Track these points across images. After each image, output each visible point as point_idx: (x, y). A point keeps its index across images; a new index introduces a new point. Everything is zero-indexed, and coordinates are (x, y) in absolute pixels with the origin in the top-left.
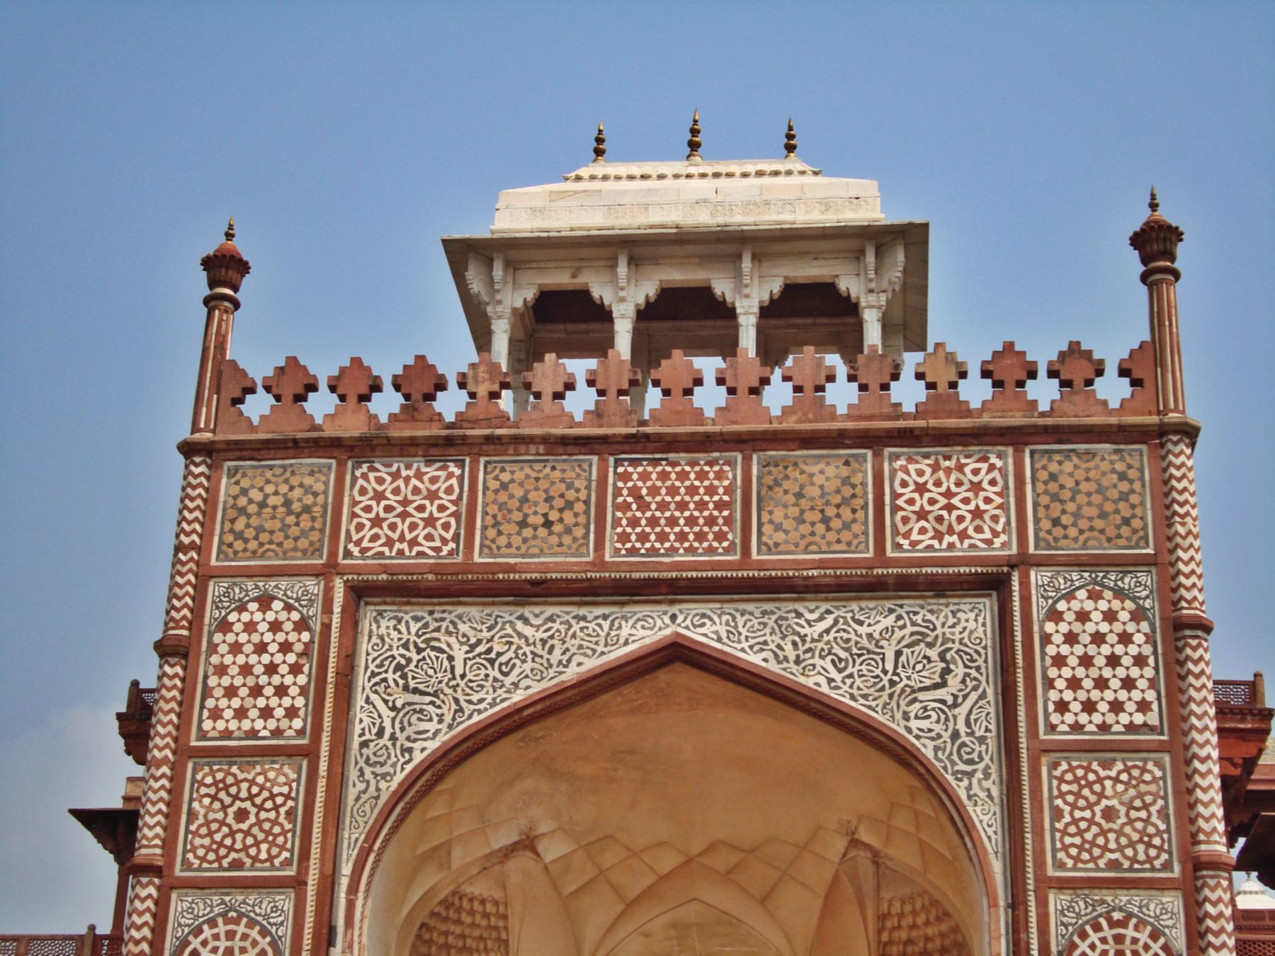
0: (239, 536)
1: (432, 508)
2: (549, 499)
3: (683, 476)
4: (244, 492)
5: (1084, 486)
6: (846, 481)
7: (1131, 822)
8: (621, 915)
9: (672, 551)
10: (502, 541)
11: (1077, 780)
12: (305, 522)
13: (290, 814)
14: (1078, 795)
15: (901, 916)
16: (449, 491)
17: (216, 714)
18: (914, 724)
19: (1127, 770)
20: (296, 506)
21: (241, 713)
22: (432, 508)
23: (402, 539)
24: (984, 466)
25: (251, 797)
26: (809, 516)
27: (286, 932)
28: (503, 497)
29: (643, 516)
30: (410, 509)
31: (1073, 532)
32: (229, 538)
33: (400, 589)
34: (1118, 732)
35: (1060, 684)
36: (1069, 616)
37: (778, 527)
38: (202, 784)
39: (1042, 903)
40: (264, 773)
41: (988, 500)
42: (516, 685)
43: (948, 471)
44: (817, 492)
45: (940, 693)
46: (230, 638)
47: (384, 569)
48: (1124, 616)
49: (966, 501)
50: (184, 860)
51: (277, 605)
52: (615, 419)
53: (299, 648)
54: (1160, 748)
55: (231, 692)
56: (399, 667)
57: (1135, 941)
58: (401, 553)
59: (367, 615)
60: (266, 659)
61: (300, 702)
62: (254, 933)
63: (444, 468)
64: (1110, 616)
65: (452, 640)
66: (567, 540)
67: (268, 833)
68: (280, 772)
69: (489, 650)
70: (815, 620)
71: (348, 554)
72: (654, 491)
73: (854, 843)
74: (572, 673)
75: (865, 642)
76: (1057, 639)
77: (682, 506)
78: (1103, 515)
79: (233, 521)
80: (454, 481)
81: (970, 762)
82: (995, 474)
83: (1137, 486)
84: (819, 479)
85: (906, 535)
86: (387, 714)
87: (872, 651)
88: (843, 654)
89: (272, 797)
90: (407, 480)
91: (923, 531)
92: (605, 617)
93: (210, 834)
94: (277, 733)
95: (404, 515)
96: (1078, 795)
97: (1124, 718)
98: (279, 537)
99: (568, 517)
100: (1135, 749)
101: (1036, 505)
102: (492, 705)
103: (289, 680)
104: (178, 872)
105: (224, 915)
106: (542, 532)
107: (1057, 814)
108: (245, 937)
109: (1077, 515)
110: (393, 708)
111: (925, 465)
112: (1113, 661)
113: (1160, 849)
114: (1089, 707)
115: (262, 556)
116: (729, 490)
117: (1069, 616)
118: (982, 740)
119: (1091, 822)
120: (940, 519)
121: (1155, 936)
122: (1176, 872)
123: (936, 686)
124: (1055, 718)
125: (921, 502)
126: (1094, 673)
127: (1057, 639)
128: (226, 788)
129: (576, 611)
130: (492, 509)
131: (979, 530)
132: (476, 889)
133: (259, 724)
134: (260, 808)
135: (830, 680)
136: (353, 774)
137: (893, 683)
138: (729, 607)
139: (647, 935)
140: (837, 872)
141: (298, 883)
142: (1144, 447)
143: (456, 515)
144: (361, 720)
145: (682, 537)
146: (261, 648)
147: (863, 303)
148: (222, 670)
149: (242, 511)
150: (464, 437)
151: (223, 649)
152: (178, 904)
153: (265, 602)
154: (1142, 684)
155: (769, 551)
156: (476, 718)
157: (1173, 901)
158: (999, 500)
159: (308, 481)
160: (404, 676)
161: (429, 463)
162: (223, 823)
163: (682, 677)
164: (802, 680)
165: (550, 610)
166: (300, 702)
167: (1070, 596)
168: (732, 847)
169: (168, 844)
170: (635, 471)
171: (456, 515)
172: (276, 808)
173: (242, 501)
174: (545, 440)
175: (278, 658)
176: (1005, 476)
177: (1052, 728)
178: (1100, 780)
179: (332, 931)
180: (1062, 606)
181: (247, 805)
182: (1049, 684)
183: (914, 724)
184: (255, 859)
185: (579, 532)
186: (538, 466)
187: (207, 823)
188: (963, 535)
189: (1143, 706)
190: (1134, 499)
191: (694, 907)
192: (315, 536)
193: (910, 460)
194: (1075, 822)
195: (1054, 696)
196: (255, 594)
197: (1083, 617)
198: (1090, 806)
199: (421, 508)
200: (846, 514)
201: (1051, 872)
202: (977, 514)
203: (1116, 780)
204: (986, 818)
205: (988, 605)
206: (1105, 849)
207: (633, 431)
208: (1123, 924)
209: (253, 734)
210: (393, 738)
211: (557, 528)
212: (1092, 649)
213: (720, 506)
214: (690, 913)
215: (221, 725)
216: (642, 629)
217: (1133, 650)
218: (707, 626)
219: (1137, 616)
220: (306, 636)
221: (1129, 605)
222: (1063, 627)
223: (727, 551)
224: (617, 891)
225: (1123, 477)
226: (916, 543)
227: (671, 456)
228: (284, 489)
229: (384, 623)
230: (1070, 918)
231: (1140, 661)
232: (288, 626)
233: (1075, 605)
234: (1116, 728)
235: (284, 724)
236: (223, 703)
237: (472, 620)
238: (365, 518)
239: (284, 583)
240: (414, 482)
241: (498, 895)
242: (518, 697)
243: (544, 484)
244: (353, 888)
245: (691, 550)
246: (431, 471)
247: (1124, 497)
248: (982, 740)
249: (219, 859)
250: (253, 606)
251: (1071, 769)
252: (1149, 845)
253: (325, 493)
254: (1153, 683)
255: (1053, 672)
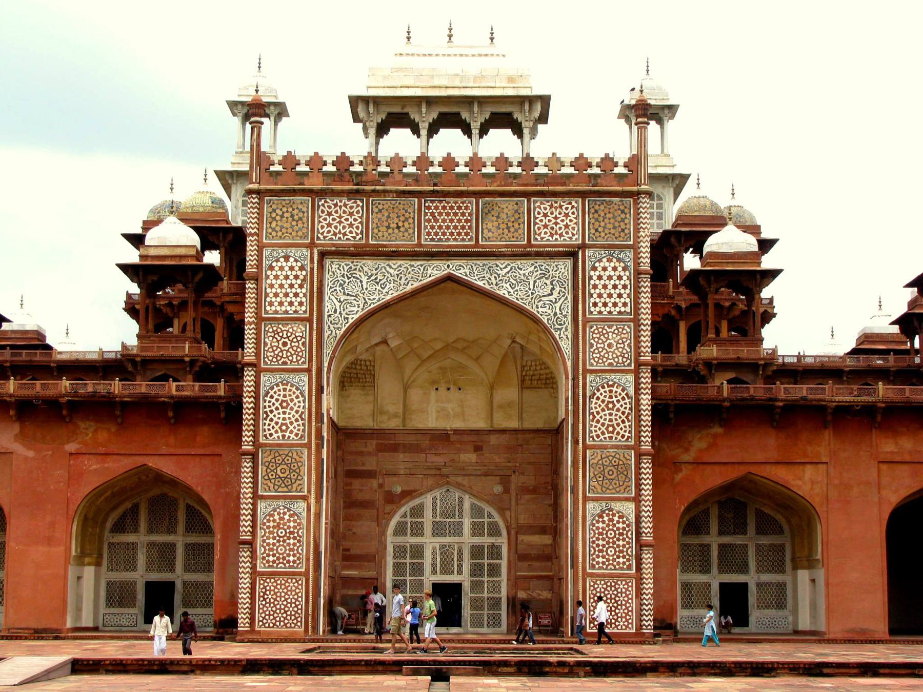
0: (274, 230)
1: (351, 220)
2: (398, 217)
3: (452, 208)
4: (274, 211)
5: (608, 215)
6: (516, 211)
7: (617, 348)
8: (419, 365)
9: (448, 240)
10: (380, 234)
11: (599, 332)
12: (300, 225)
13: (304, 344)
14: (599, 338)
15: (531, 366)
16: (358, 212)
17: (271, 304)
18: (540, 310)
19: (617, 329)
20: (296, 218)
21: (281, 304)
22: (351, 220)
23: (340, 232)
24: (570, 206)
25: (288, 337)
26: (502, 226)
27: (306, 388)
28: (379, 216)
29: (436, 225)
30: (343, 220)
31: (603, 234)
32: (270, 230)
33: (341, 253)
34: (615, 316)
35: (595, 296)
36: (600, 269)
37: (490, 231)
38: (268, 331)
39: (584, 379)
40: (292, 328)
41: (571, 221)
42: (387, 293)
43: (556, 208)
44: (505, 217)
45: (551, 298)
46: (274, 273)
47: (334, 245)
48: (620, 269)
49: (562, 221)
50: (264, 361)
51: (292, 259)
52: (425, 183)
53: (301, 277)
54: (630, 320)
55: (276, 295)
56: (341, 285)
57: (616, 392)
58: (340, 238)
59: (328, 262)
60: (289, 281)
61: (304, 300)
62: (294, 389)
63: (355, 202)
64: (615, 269)
65: (361, 274)
66: (406, 234)
67: (296, 351)
68: (298, 327)
69: (376, 279)
70: (503, 267)
71: (318, 238)
72: (440, 214)
73: (514, 342)
74: (409, 288)
75: (522, 277)
76: (595, 278)
77: (452, 221)
78: (614, 228)
79: (270, 223)
80: (359, 208)
81: (561, 325)
82: (574, 210)
83: (628, 216)
84: (506, 211)
85: (539, 235)
86: (338, 304)
87: (524, 281)
88: (514, 282)
89: (296, 337)
90: (341, 207)
91: (546, 233)
92: (422, 265)
93: (273, 351)
94: (296, 312)
95: (340, 222)
96: (599, 338)
97: (618, 309)
98: (290, 230)
99: (406, 224)
100: (621, 321)
101: (589, 223)
102: (379, 300)
103: (299, 290)
104: (262, 366)
105: (282, 382)
106: (396, 231)
107: (591, 345)
108: (290, 390)
109: (604, 228)
110: (340, 301)
111: (547, 205)
112: (615, 287)
113: (627, 358)
114: (605, 305)
115: (284, 238)
116: (470, 215)
117: (600, 269)
118: (565, 316)
119: (603, 348)
120: (552, 228)
121: (623, 390)
122: (633, 367)
123: (549, 295)
124: (592, 309)
125: (545, 221)
126: (608, 291)
127: (595, 278)
128: (278, 334)
129: (410, 263)
130: (376, 221)
131: (567, 233)
132: (363, 357)
133: (288, 308)
134: (292, 341)
135: (509, 292)
136: (326, 328)
137: (532, 294)
138: (470, 262)
139: (430, 372)
140: (506, 353)
141: (309, 370)
142: (631, 200)
143: (361, 223)
144: (328, 306)
145: (452, 234)
146: (287, 277)
147: (523, 125)
148: (272, 286)
149: (274, 219)
150: (363, 190)
151: (271, 277)
152: (264, 378)
153: (287, 258)
154: (625, 296)
155: (486, 241)
156: (372, 306)
157: (631, 378)
158: (575, 221)
159: (300, 207)
160: (343, 289)
161: (349, 200)
162: (278, 347)
163: (450, 285)
164: (498, 292)
165: (400, 262)
166: (304, 300)
167: (600, 261)
168: (465, 340)
169: (258, 355)
170: (433, 205)
171: (361, 223)
172: (298, 341)
173: (274, 215)
174: (396, 192)
175: (294, 282)
176: (578, 211)
177: (592, 313)
178: (607, 333)
179: (322, 388)
180: (597, 264)
181: (286, 340)
182: (591, 295)
183: (540, 310)
184: (291, 361)
185: (411, 231)
186: (393, 202)
187: (272, 347)
188: (561, 235)
189: (625, 305)
190: (626, 221)
191: (448, 361)
192: (305, 230)
193: (542, 203)
194: (598, 348)
195: (592, 300)
196: (282, 254)
197: (605, 269)
198: (603, 343)
199: (347, 220)
200: (516, 226)
201: (588, 367)
202: (567, 226)
203: (613, 333)
204: (566, 346)
205: (569, 262)
206: (608, 359)
207: (432, 188)
208: (612, 386)
209: (286, 312)
210: (340, 313)
211: (402, 229)
212: (607, 282)
213: (467, 221)
214: (447, 363)
215: (273, 308)
216: (436, 270)
217: (622, 282)
218: (462, 269)
219: (624, 269)
220: (304, 273)
221: (622, 265)
222: (597, 273)
223: (470, 240)
224: (419, 356)
225: (623, 212)
226: (543, 238)
227: (447, 199)
228: (290, 210)
229: (334, 266)
230: (594, 384)
231: (625, 287)
232: (297, 268)
233: (602, 264)
234: (615, 313)
235: (298, 308)
236: (273, 300)
237: (369, 264)
238: (324, 223)
239: (294, 250)
240: (343, 208)
241: (371, 358)
242: (389, 297)
243: (396, 210)
244: (329, 372)
245: (455, 240)
246: (350, 203)
247: (623, 220)
248: (565, 316)
249: (277, 361)
250: (282, 260)
251: (597, 329)
252: (623, 357)
253: (308, 212)
254: (629, 296)
255: (592, 291)
